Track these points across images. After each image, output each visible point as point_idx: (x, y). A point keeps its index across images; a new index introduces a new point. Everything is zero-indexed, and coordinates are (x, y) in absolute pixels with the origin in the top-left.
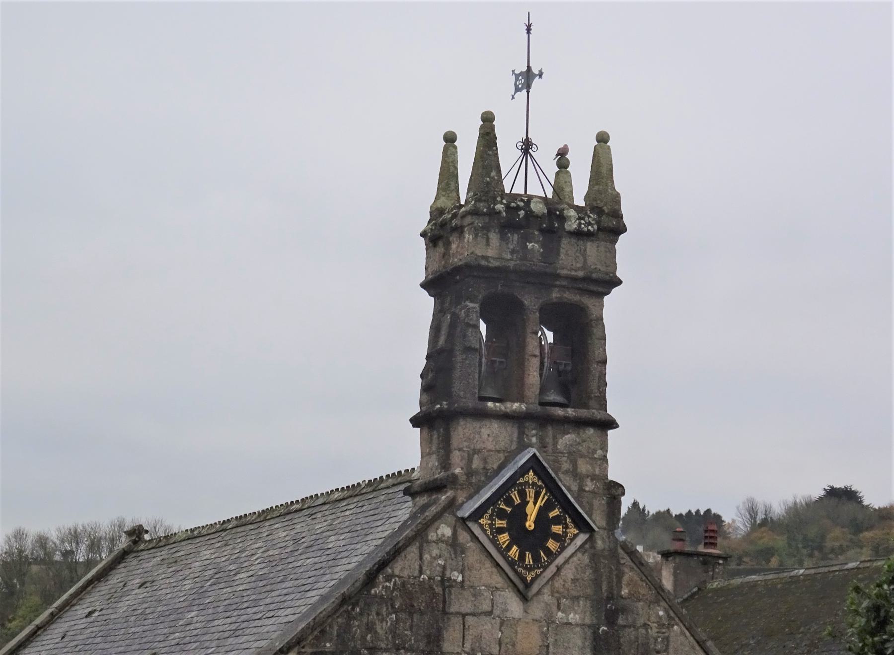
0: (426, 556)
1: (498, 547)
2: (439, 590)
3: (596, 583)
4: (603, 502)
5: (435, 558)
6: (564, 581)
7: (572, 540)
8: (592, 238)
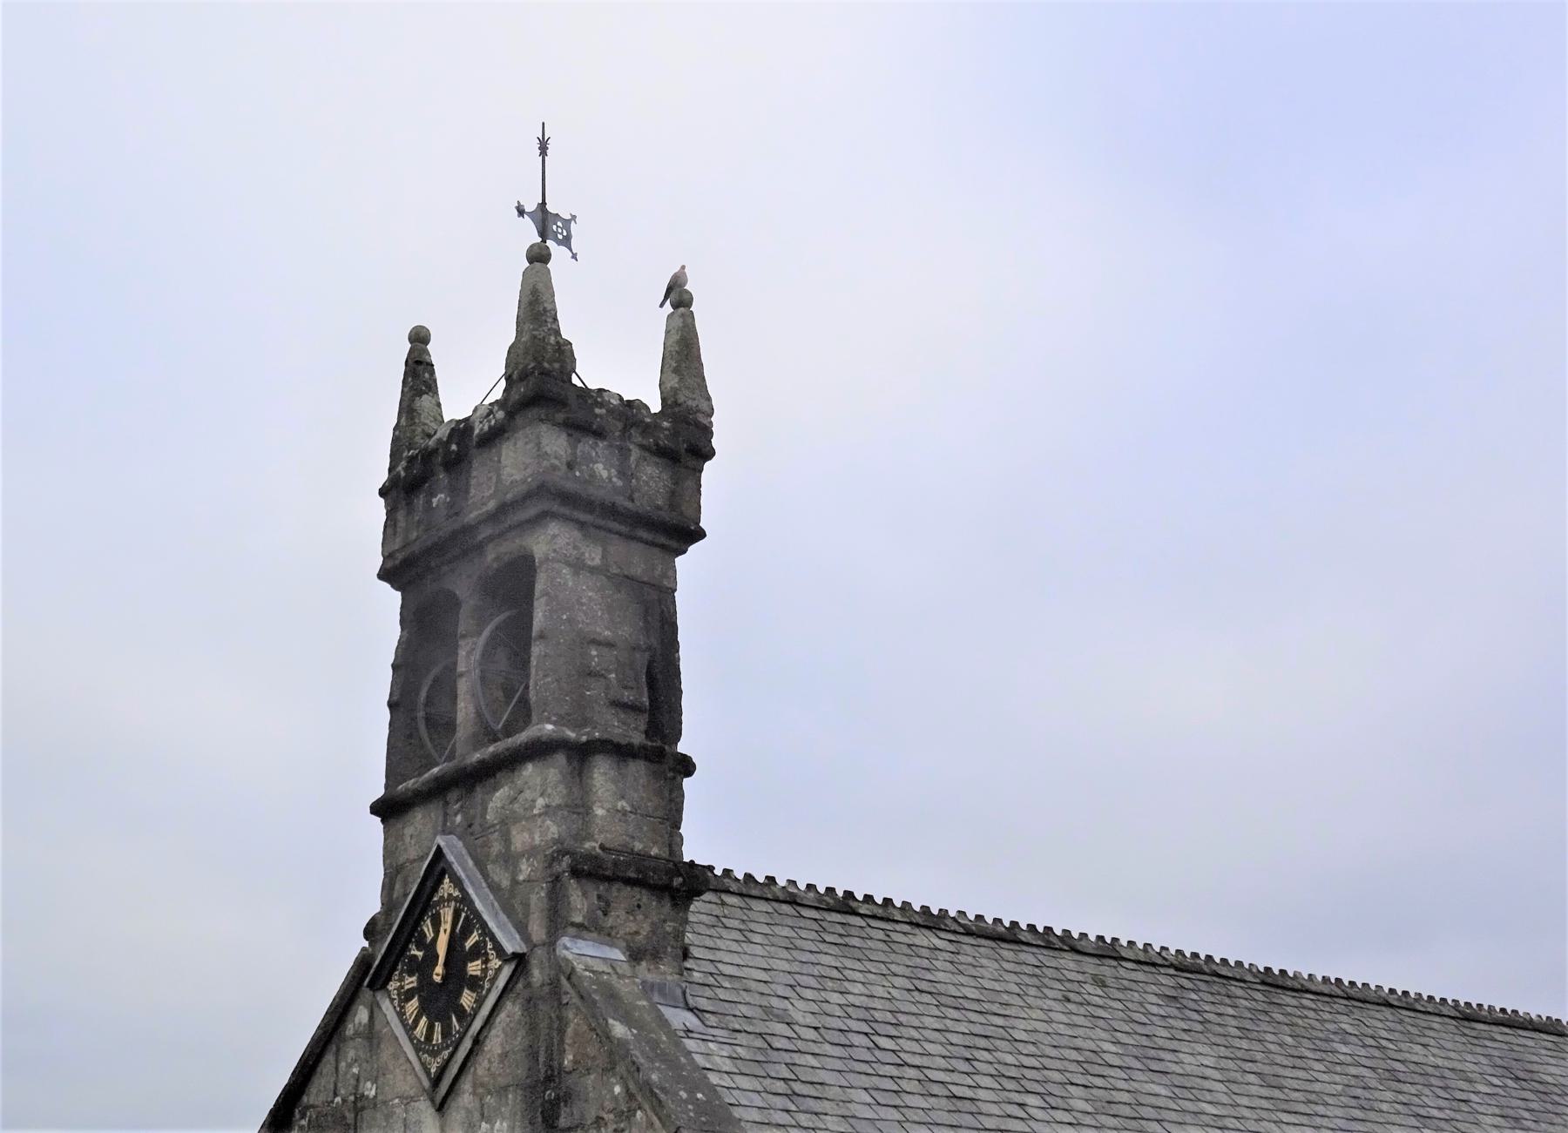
0: (343, 1065)
1: (403, 1022)
2: (350, 1116)
3: (533, 1055)
4: (543, 894)
5: (350, 1066)
6: (490, 1062)
7: (493, 980)
8: (506, 435)
